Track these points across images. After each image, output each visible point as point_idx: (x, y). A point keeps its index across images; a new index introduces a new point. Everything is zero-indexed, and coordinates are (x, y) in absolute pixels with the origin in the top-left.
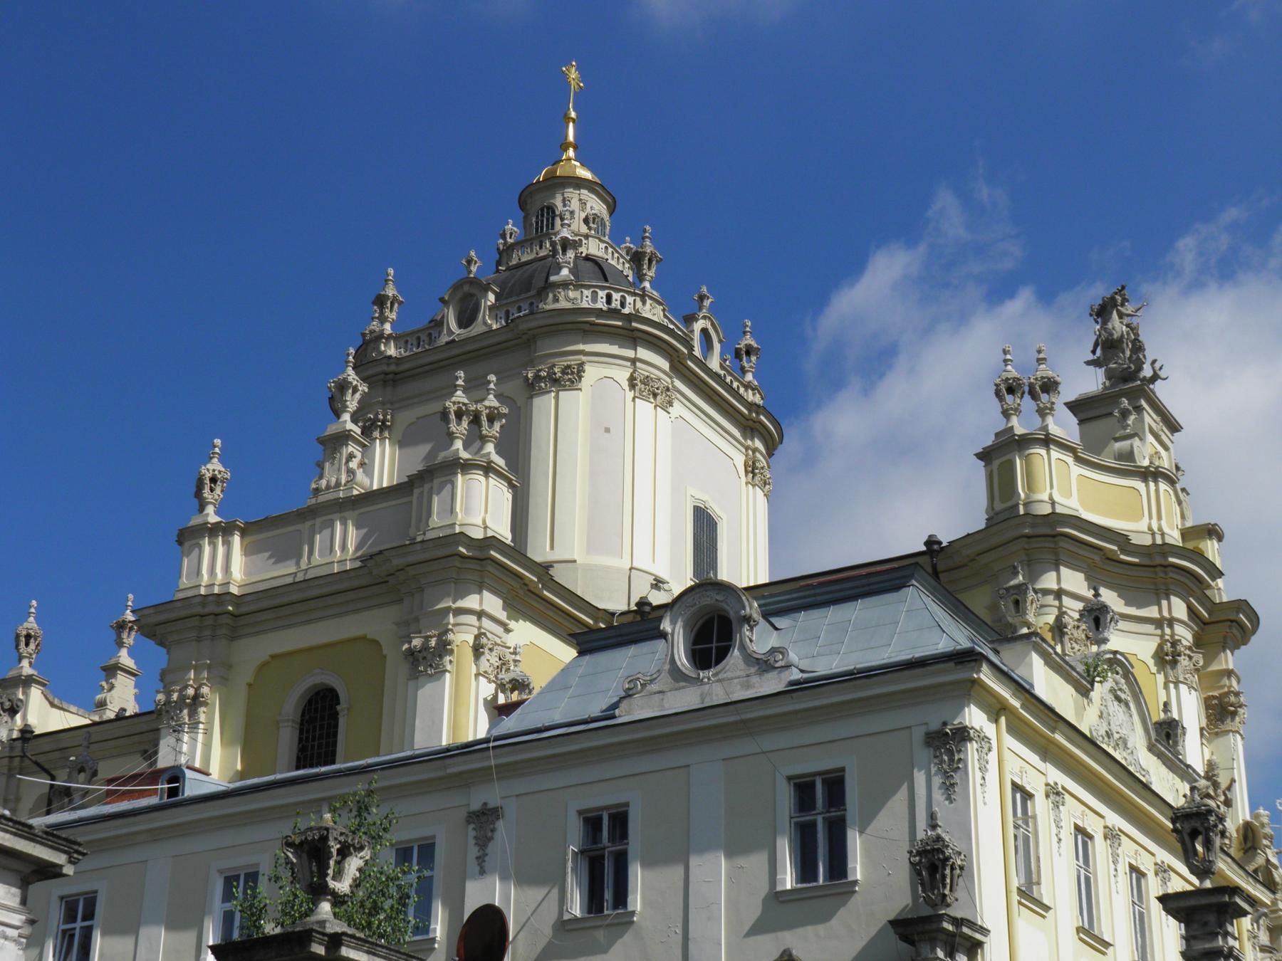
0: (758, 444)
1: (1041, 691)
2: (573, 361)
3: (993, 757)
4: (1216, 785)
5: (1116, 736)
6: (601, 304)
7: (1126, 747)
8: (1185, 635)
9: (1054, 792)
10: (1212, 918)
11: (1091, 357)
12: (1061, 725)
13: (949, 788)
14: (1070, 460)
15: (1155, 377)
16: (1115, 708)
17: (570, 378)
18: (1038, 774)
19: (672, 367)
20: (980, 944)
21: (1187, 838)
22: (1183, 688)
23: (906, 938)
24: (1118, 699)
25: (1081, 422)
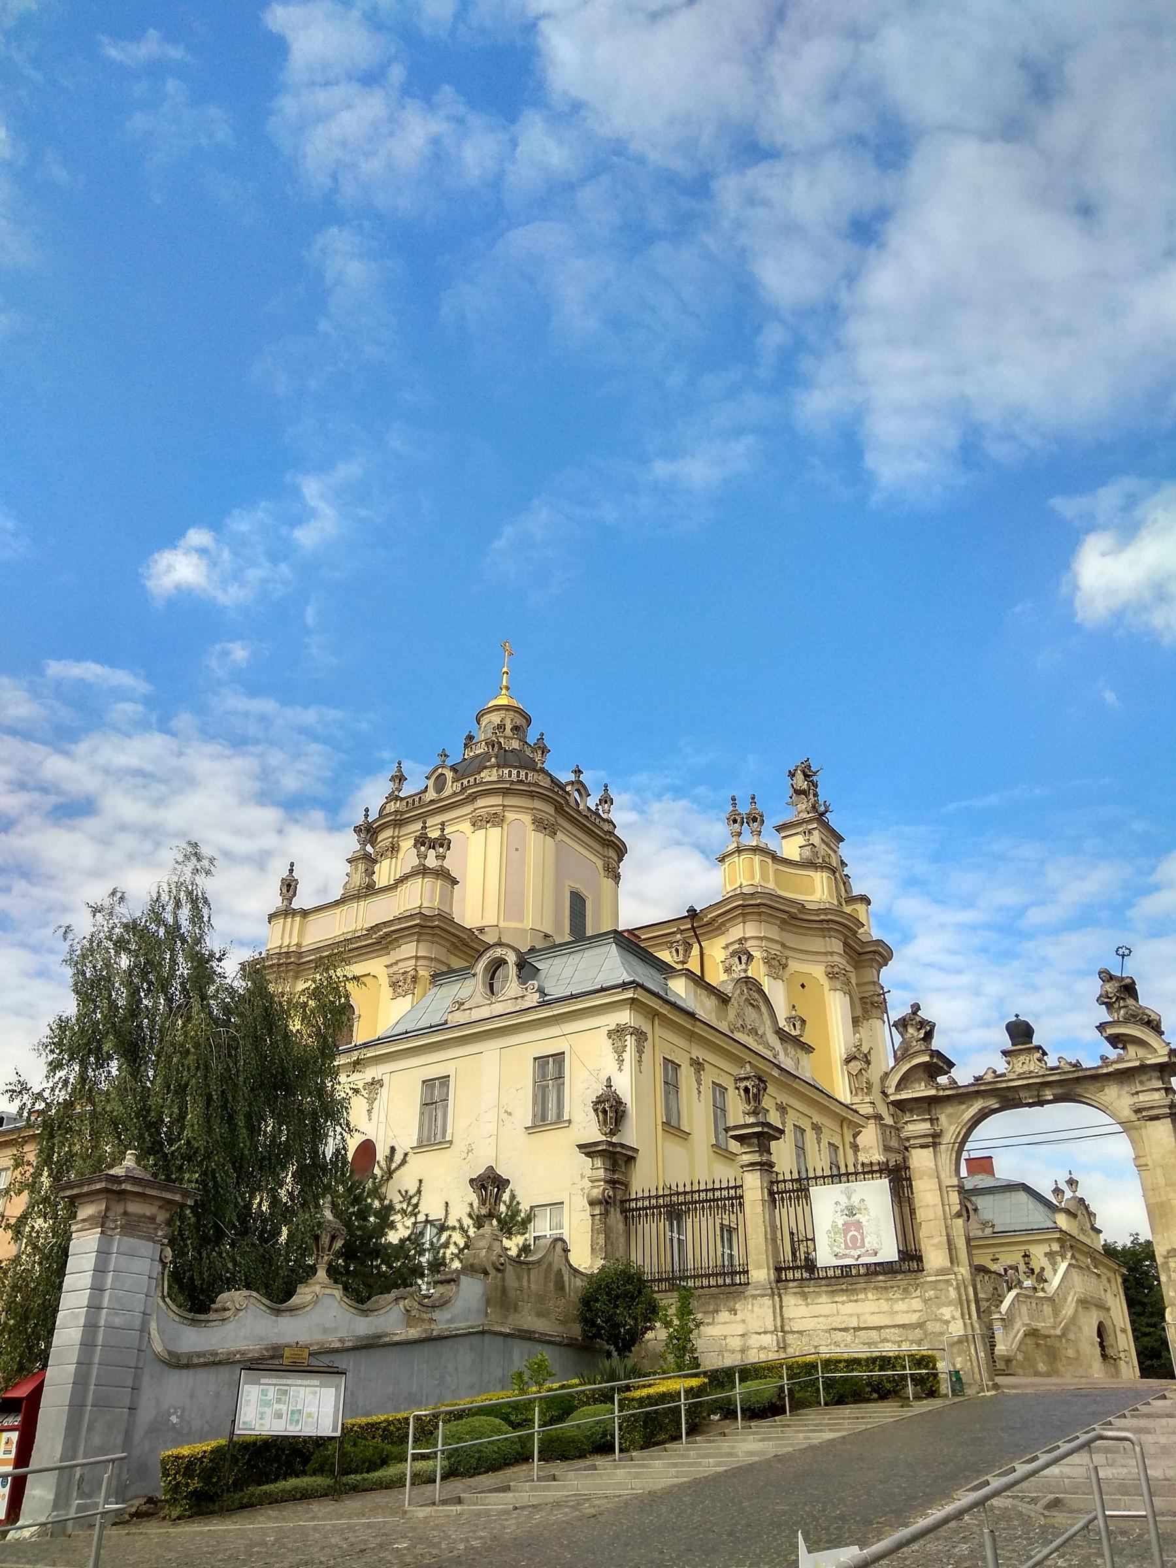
0: (612, 854)
2: (499, 810)
3: (648, 1045)
6: (514, 778)
7: (757, 1034)
8: (840, 961)
9: (698, 1065)
10: (755, 1141)
12: (698, 1023)
14: (770, 861)
16: (749, 1011)
17: (496, 819)
18: (682, 1051)
20: (633, 1158)
23: (588, 1154)
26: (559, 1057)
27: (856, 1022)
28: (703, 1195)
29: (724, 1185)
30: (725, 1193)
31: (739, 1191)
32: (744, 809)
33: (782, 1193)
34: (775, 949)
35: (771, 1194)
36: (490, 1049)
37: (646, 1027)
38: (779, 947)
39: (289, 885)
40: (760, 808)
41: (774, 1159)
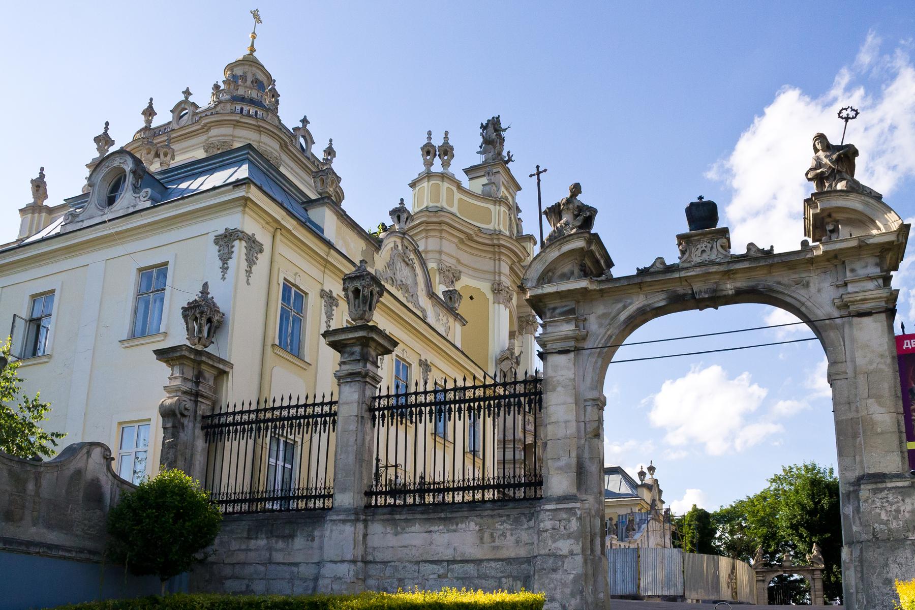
1: (329, 234)
4: (512, 354)
5: (399, 282)
7: (407, 291)
10: (357, 349)
11: (479, 149)
12: (332, 251)
13: (225, 269)
14: (455, 189)
15: (510, 160)
16: (400, 265)
19: (281, 147)
20: (226, 373)
21: (351, 295)
22: (502, 306)
24: (407, 264)
25: (471, 179)
26: (162, 268)
27: (512, 335)
28: (293, 412)
29: (319, 400)
30: (318, 410)
31: (334, 408)
32: (437, 142)
33: (384, 409)
34: (449, 262)
35: (372, 410)
36: (96, 259)
37: (263, 237)
38: (453, 261)
39: (38, 186)
40: (451, 142)
41: (380, 372)
